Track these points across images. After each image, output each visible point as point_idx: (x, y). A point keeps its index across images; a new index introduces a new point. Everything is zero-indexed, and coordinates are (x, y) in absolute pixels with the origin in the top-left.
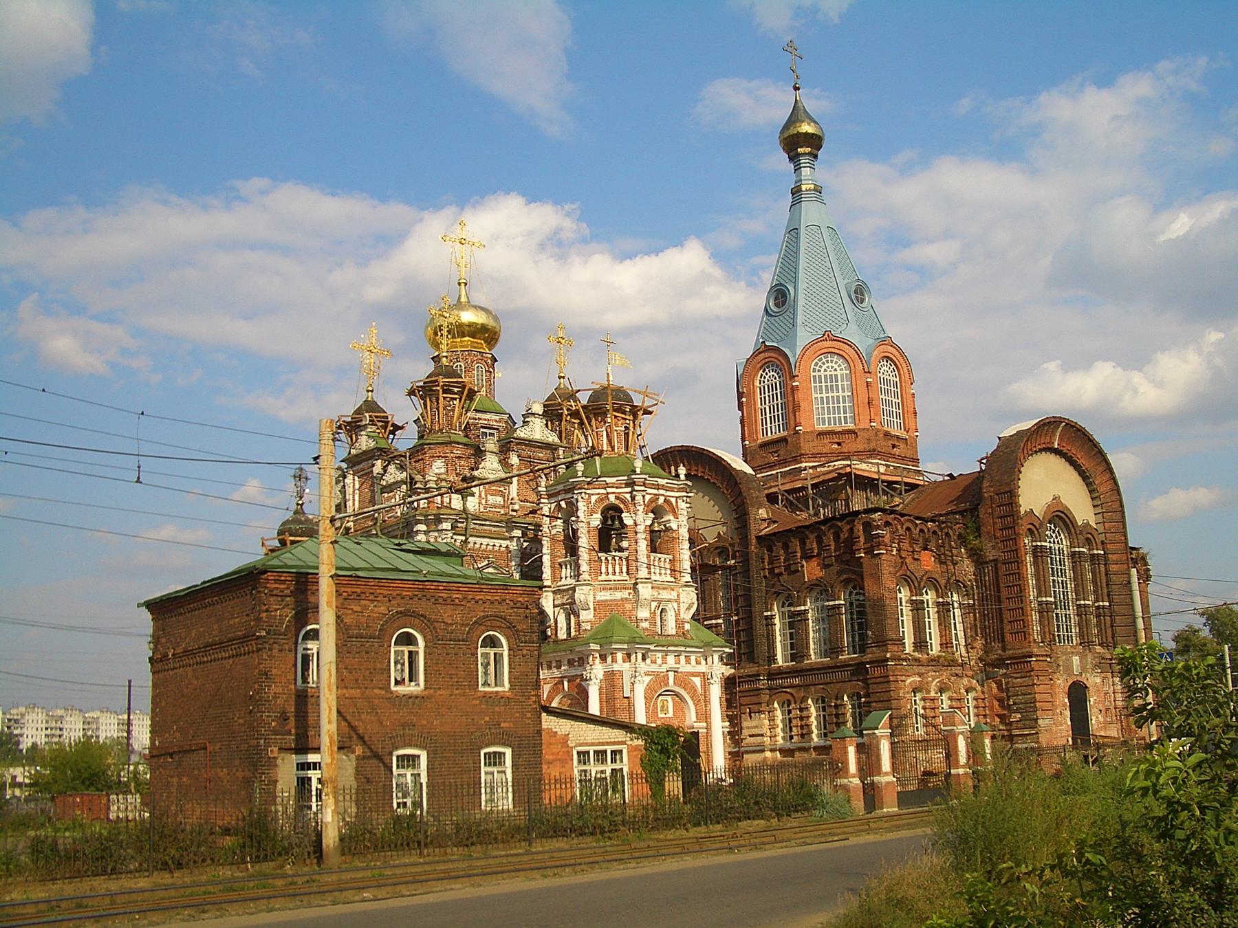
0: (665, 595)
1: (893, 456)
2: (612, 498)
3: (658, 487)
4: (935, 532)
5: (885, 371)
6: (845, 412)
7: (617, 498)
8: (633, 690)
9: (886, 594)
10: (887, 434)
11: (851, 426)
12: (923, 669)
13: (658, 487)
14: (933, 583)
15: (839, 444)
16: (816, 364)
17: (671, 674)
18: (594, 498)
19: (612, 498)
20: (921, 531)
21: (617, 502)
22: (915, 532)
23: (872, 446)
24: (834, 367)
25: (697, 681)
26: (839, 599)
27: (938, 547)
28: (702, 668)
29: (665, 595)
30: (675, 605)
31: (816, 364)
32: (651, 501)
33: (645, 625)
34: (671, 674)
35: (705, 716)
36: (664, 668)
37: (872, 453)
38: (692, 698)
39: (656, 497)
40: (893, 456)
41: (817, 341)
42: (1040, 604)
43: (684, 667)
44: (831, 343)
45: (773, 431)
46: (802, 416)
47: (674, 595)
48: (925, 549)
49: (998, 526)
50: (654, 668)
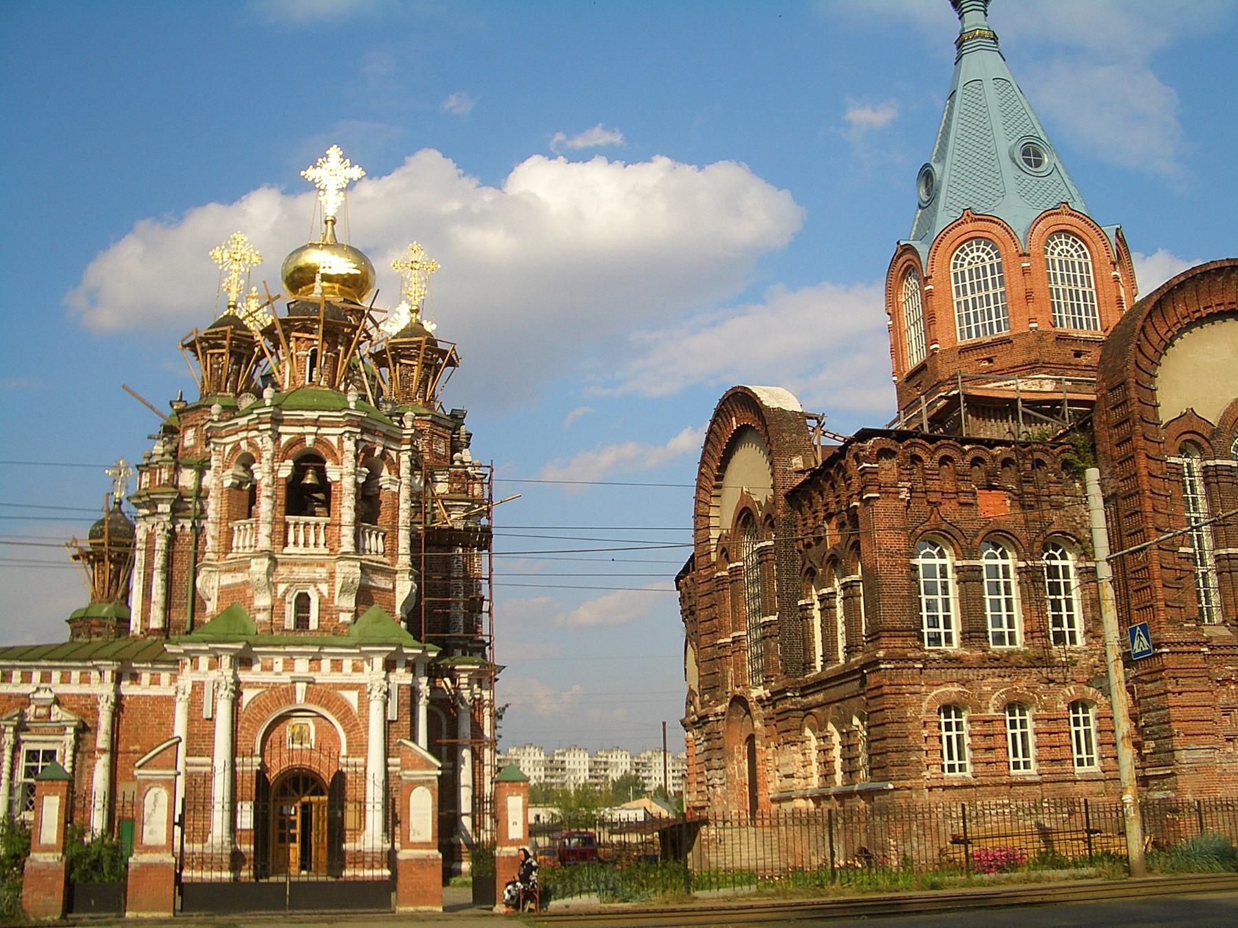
0: (303, 573)
1: (1076, 367)
2: (243, 444)
3: (303, 423)
4: (1006, 462)
5: (1062, 249)
6: (998, 316)
7: (250, 444)
8: (214, 711)
9: (882, 560)
10: (1061, 338)
11: (1005, 333)
12: (971, 675)
13: (303, 423)
14: (998, 538)
15: (990, 360)
16: (957, 258)
17: (301, 688)
18: (228, 448)
19: (243, 444)
20: (976, 461)
21: (250, 450)
22: (963, 464)
23: (1033, 356)
24: (978, 256)
25: (352, 697)
26: (854, 572)
27: (1020, 482)
28: (357, 678)
29: (303, 573)
30: (324, 588)
31: (957, 258)
32: (291, 444)
33: (263, 616)
34: (301, 688)
35: (358, 747)
36: (286, 678)
37: (1033, 367)
38: (341, 721)
39: (301, 439)
40: (1076, 367)
41: (957, 223)
42: (1218, 558)
43: (325, 675)
44: (978, 227)
45: (914, 359)
46: (939, 330)
47: (322, 572)
48: (990, 487)
49: (1116, 438)
50: (268, 677)
